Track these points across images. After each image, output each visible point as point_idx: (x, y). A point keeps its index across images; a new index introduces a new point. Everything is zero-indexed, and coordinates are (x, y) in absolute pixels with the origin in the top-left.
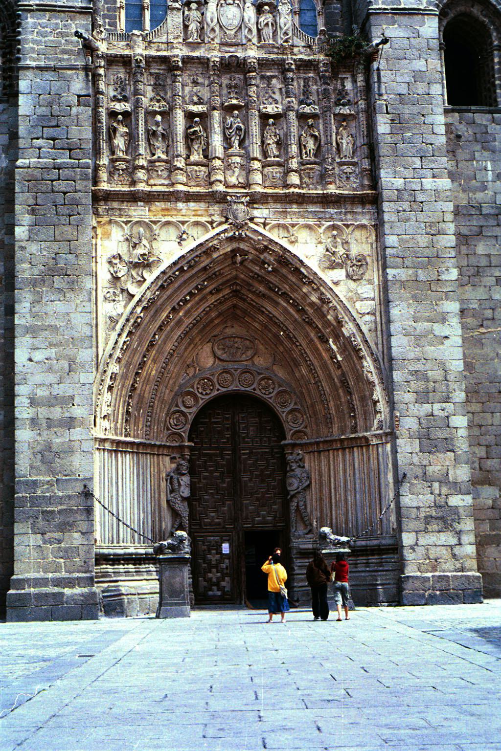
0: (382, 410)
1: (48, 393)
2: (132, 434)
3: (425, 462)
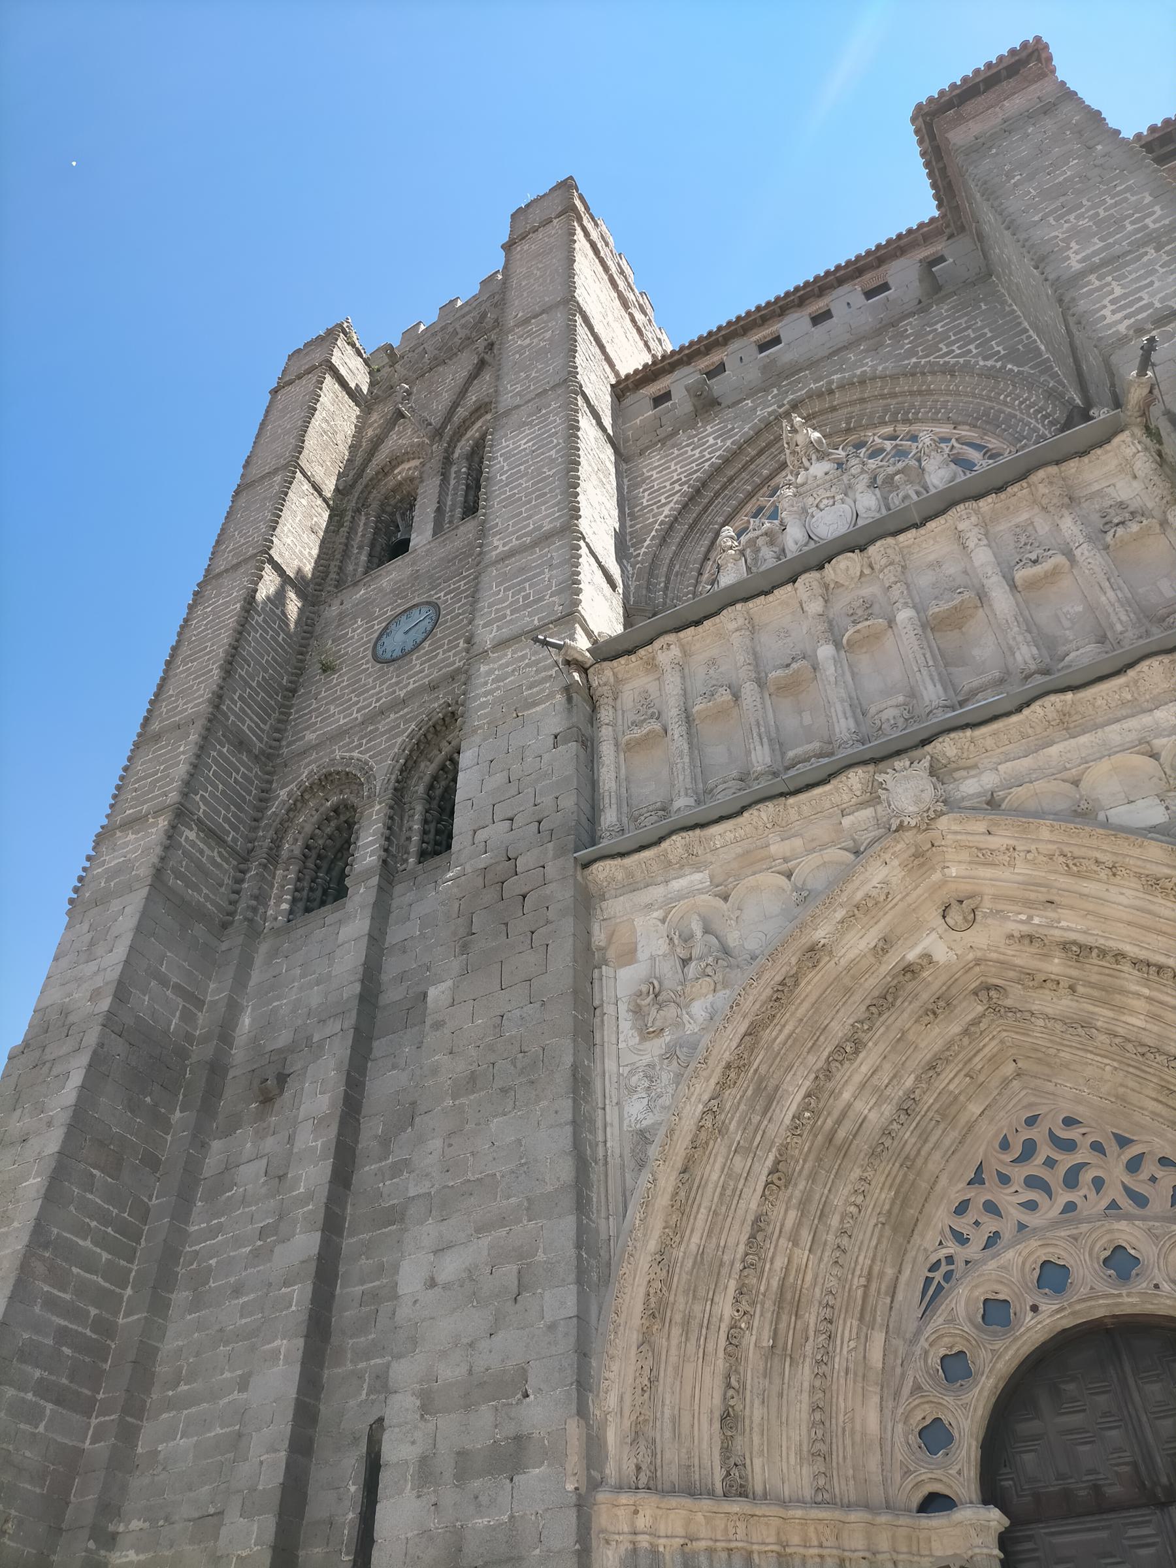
1: (463, 1370)
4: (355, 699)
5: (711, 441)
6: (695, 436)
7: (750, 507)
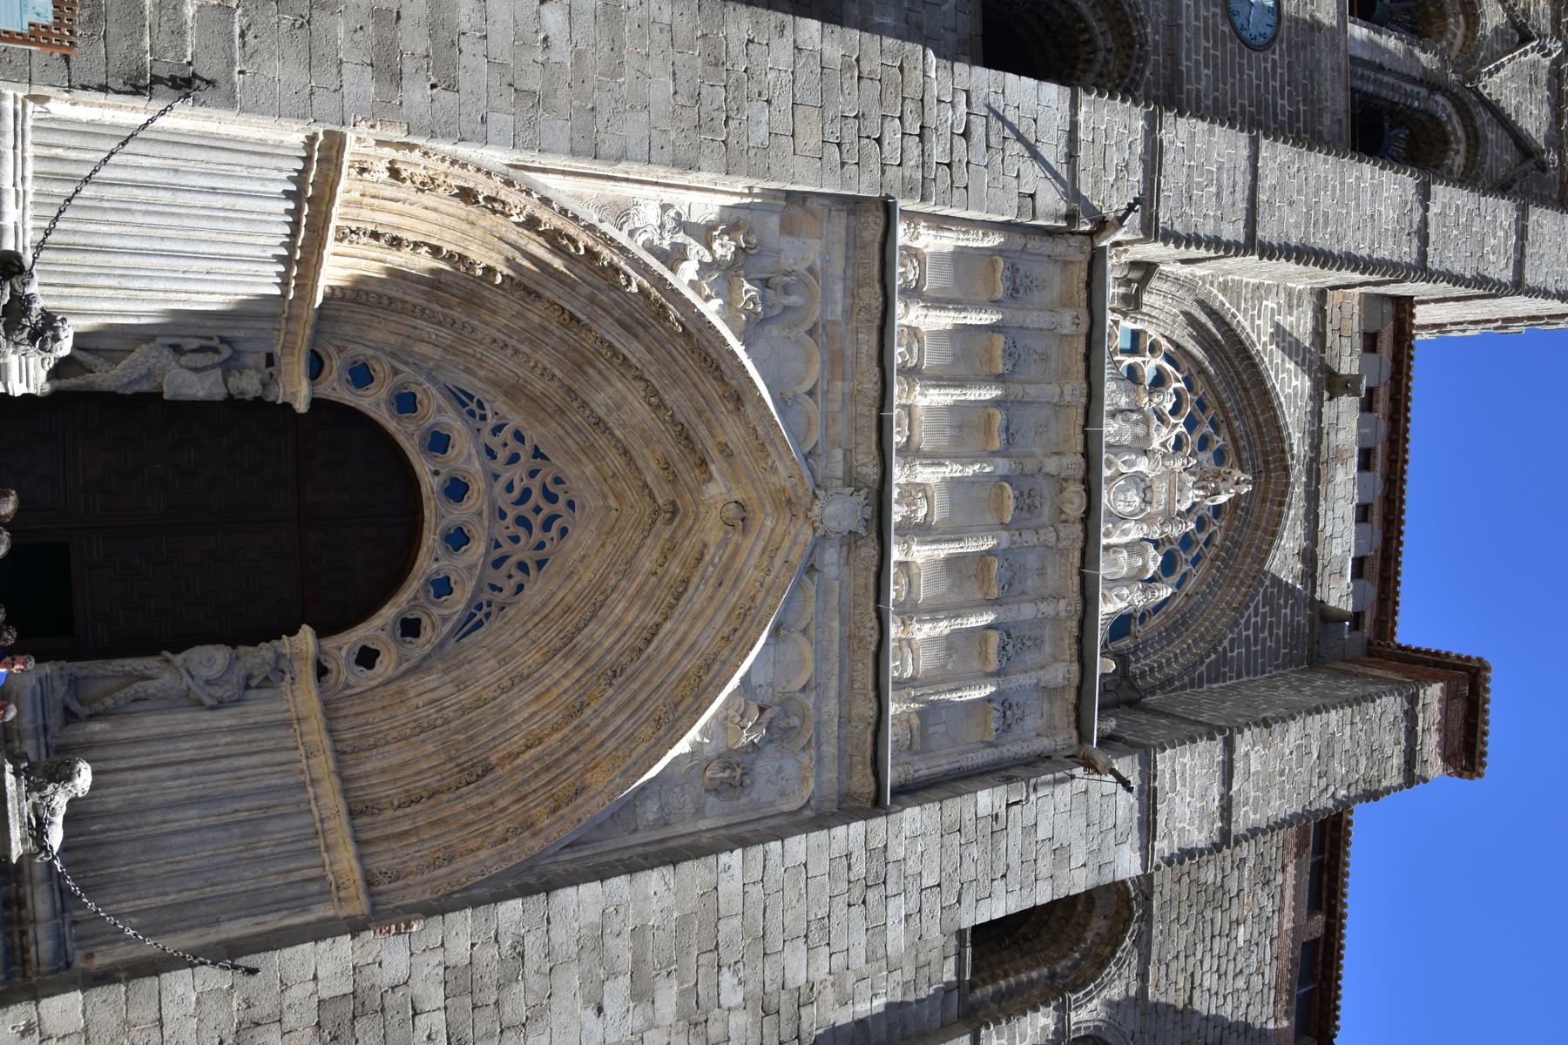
1: (465, 26)
3: (290, 1020)
5: (1294, 383)
7: (1210, 399)
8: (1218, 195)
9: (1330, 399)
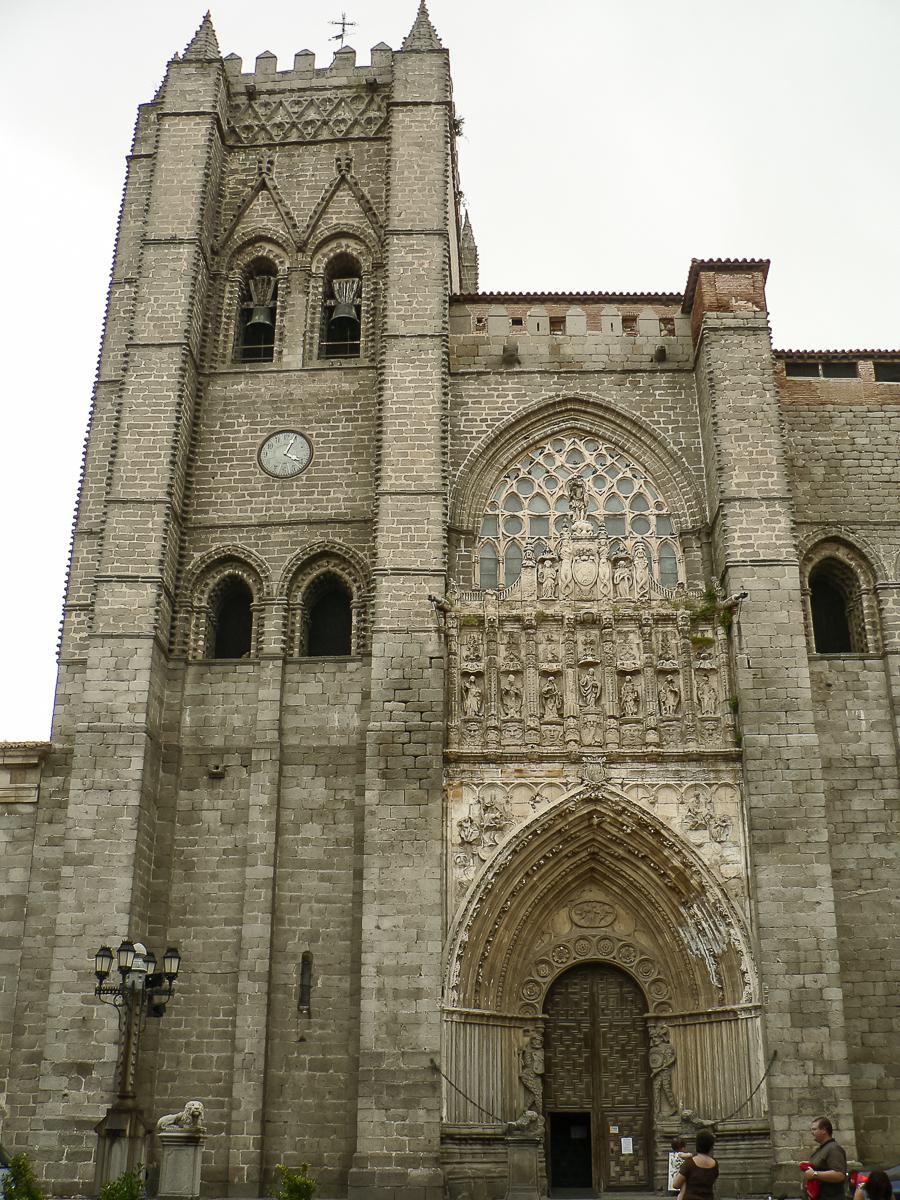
0: (751, 982)
1: (395, 962)
2: (482, 1006)
3: (798, 1039)
4: (248, 498)
6: (501, 384)
7: (520, 458)
8: (415, 522)
9: (519, 363)
